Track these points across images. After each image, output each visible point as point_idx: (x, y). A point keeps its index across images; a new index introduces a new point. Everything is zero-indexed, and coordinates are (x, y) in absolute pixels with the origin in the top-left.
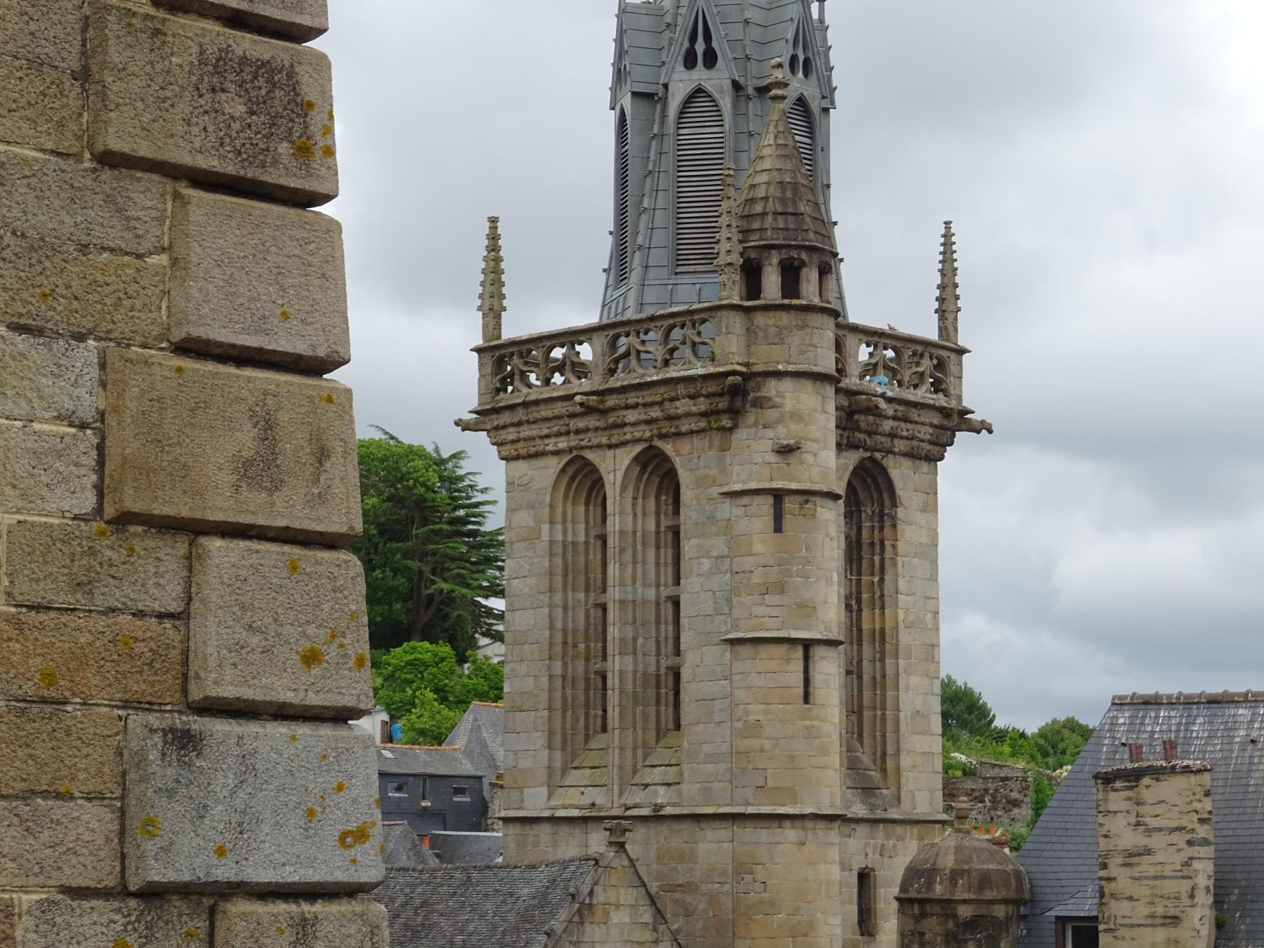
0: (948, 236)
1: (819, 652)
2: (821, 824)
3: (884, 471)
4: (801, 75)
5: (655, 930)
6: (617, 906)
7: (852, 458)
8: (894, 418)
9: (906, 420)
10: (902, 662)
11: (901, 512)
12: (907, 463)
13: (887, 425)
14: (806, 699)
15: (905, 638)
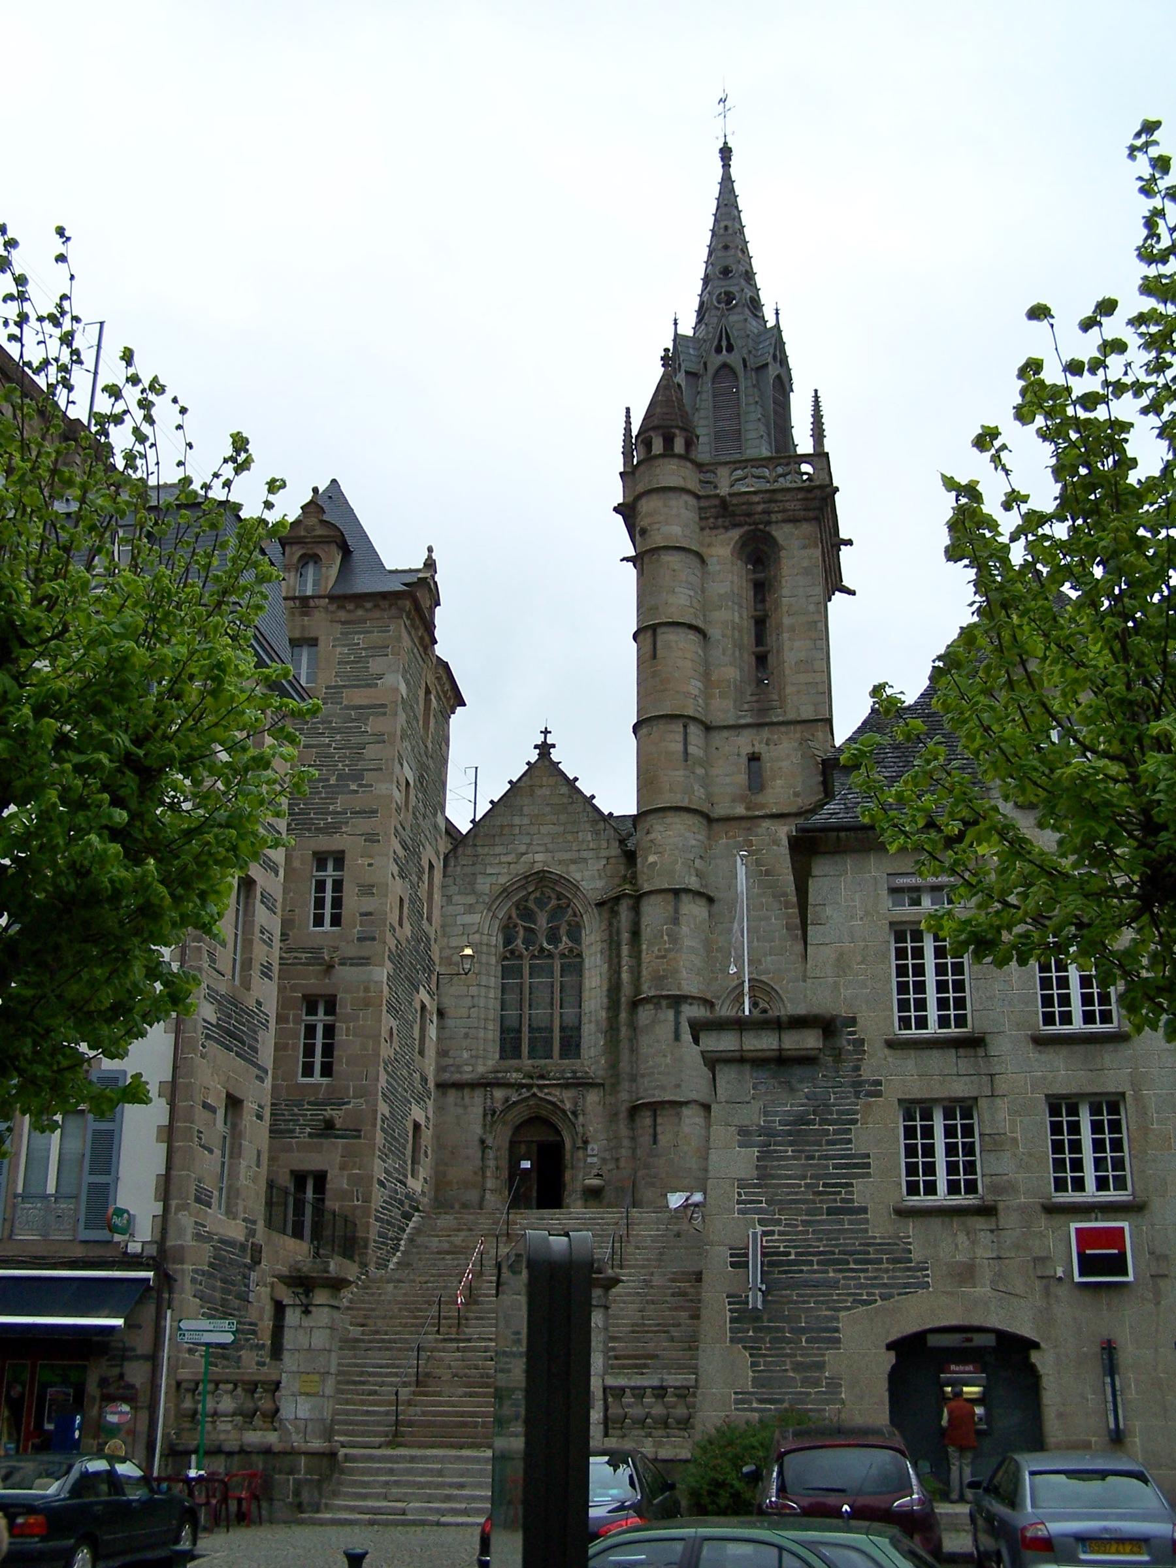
0: (816, 397)
1: (660, 630)
2: (662, 722)
3: (769, 534)
4: (724, 352)
5: (570, 797)
6: (541, 786)
7: (735, 534)
8: (764, 503)
9: (776, 501)
10: (786, 635)
11: (783, 553)
12: (788, 528)
13: (760, 508)
14: (654, 656)
15: (787, 621)
